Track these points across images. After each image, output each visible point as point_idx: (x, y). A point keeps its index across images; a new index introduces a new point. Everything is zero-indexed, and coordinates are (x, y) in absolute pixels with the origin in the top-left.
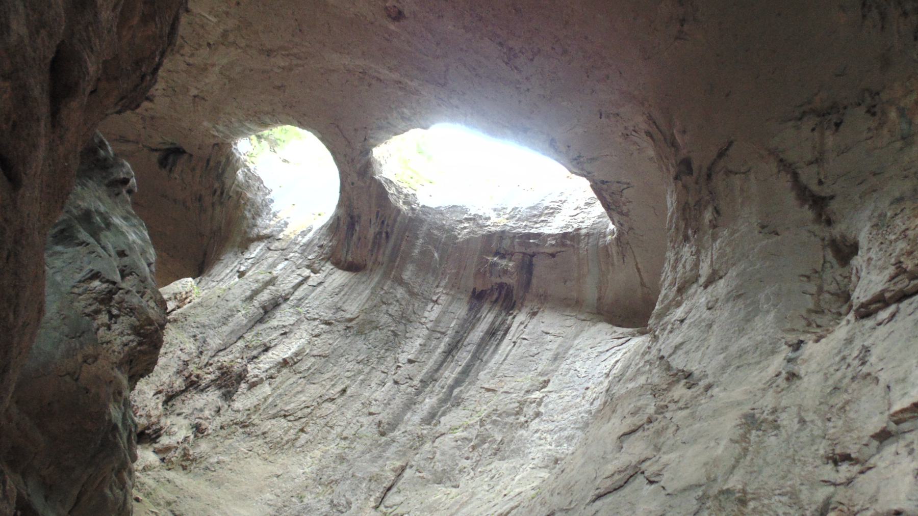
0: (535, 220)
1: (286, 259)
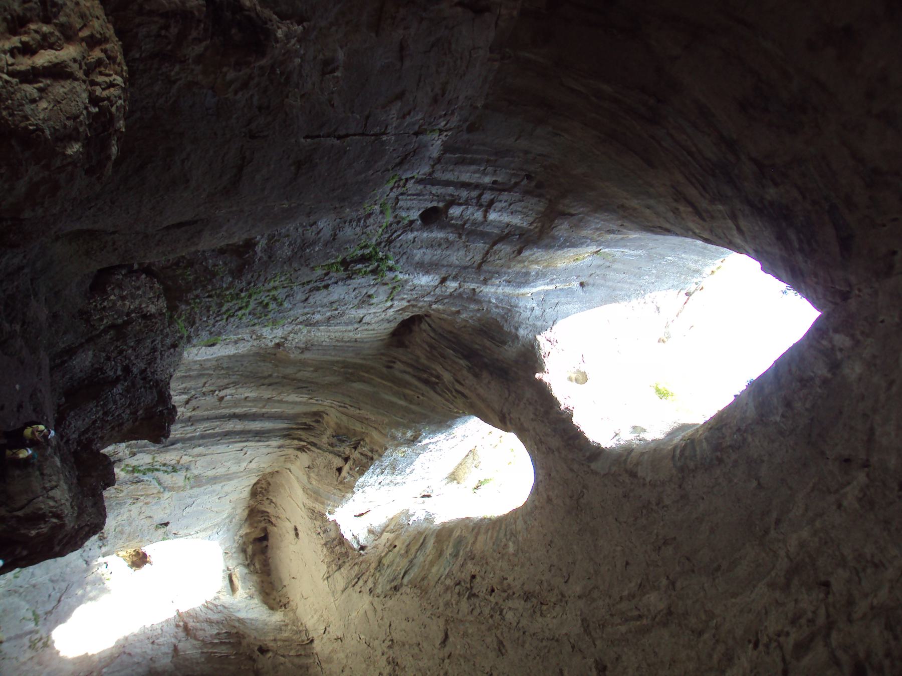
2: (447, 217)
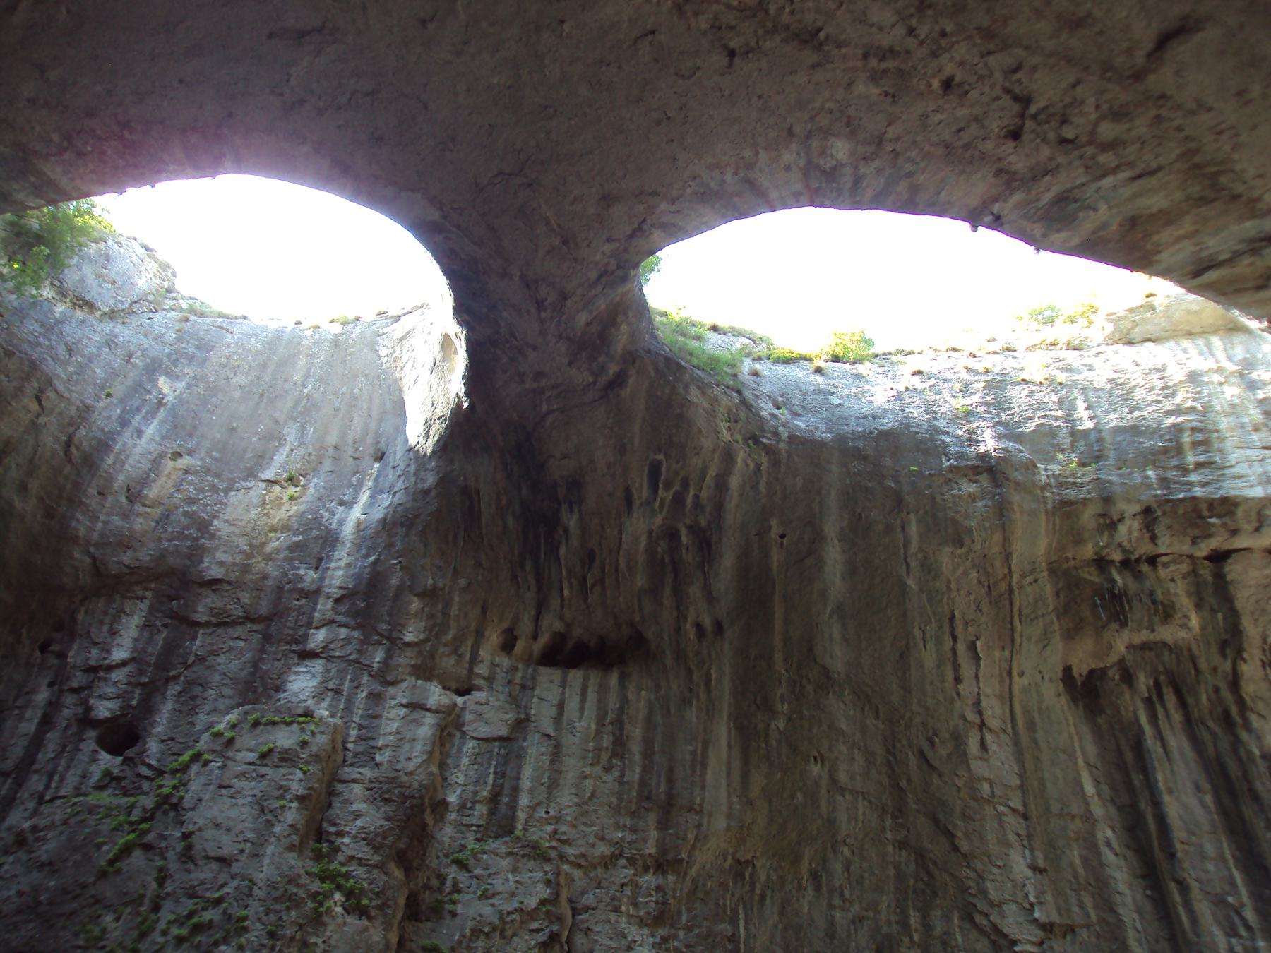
0: (1175, 462)
1: (313, 655)
2: (123, 715)
